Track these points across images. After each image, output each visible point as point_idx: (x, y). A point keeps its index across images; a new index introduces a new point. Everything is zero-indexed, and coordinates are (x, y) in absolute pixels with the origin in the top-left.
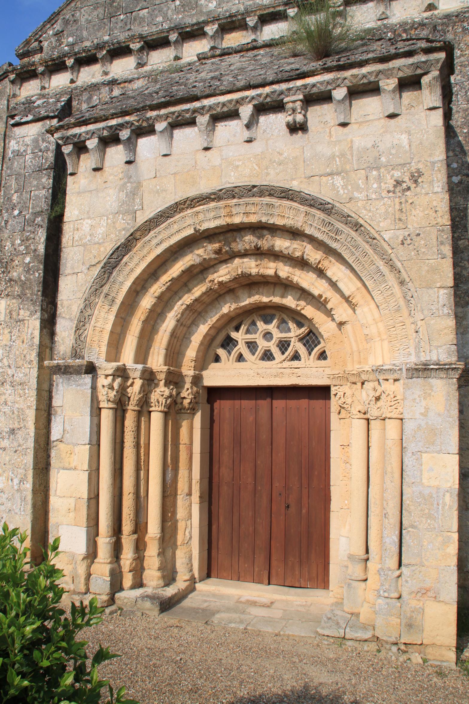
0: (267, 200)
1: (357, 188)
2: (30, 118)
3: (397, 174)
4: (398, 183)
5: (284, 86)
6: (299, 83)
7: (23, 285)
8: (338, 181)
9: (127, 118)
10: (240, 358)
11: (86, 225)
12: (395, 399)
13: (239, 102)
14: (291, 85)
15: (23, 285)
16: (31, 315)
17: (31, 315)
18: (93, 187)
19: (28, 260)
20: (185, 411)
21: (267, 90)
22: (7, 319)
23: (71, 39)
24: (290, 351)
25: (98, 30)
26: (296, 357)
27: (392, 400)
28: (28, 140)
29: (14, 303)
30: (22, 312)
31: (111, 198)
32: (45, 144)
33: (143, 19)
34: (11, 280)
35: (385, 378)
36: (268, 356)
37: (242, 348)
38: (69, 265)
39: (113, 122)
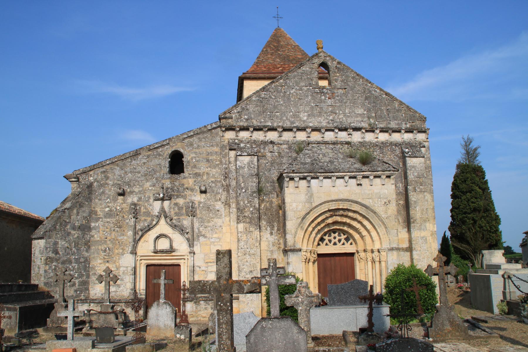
0: (350, 203)
1: (375, 203)
2: (246, 154)
3: (385, 200)
4: (385, 203)
5: (358, 173)
6: (362, 173)
7: (250, 218)
8: (371, 201)
9: (310, 174)
10: (327, 244)
11: (294, 205)
13: (345, 175)
14: (360, 173)
15: (250, 218)
16: (255, 229)
17: (255, 229)
18: (295, 192)
19: (251, 209)
21: (353, 174)
22: (245, 230)
23: (246, 117)
24: (342, 242)
25: (259, 116)
26: (343, 244)
28: (245, 162)
29: (248, 225)
30: (251, 228)
31: (303, 197)
32: (253, 166)
33: (277, 117)
34: (245, 216)
36: (335, 244)
37: (326, 241)
38: (289, 217)
39: (306, 174)
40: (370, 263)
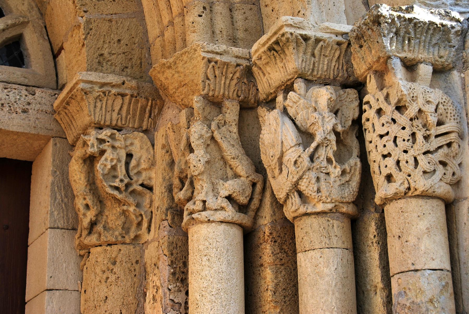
12: (442, 129)
27: (434, 131)
35: (410, 55)
40: (214, 253)
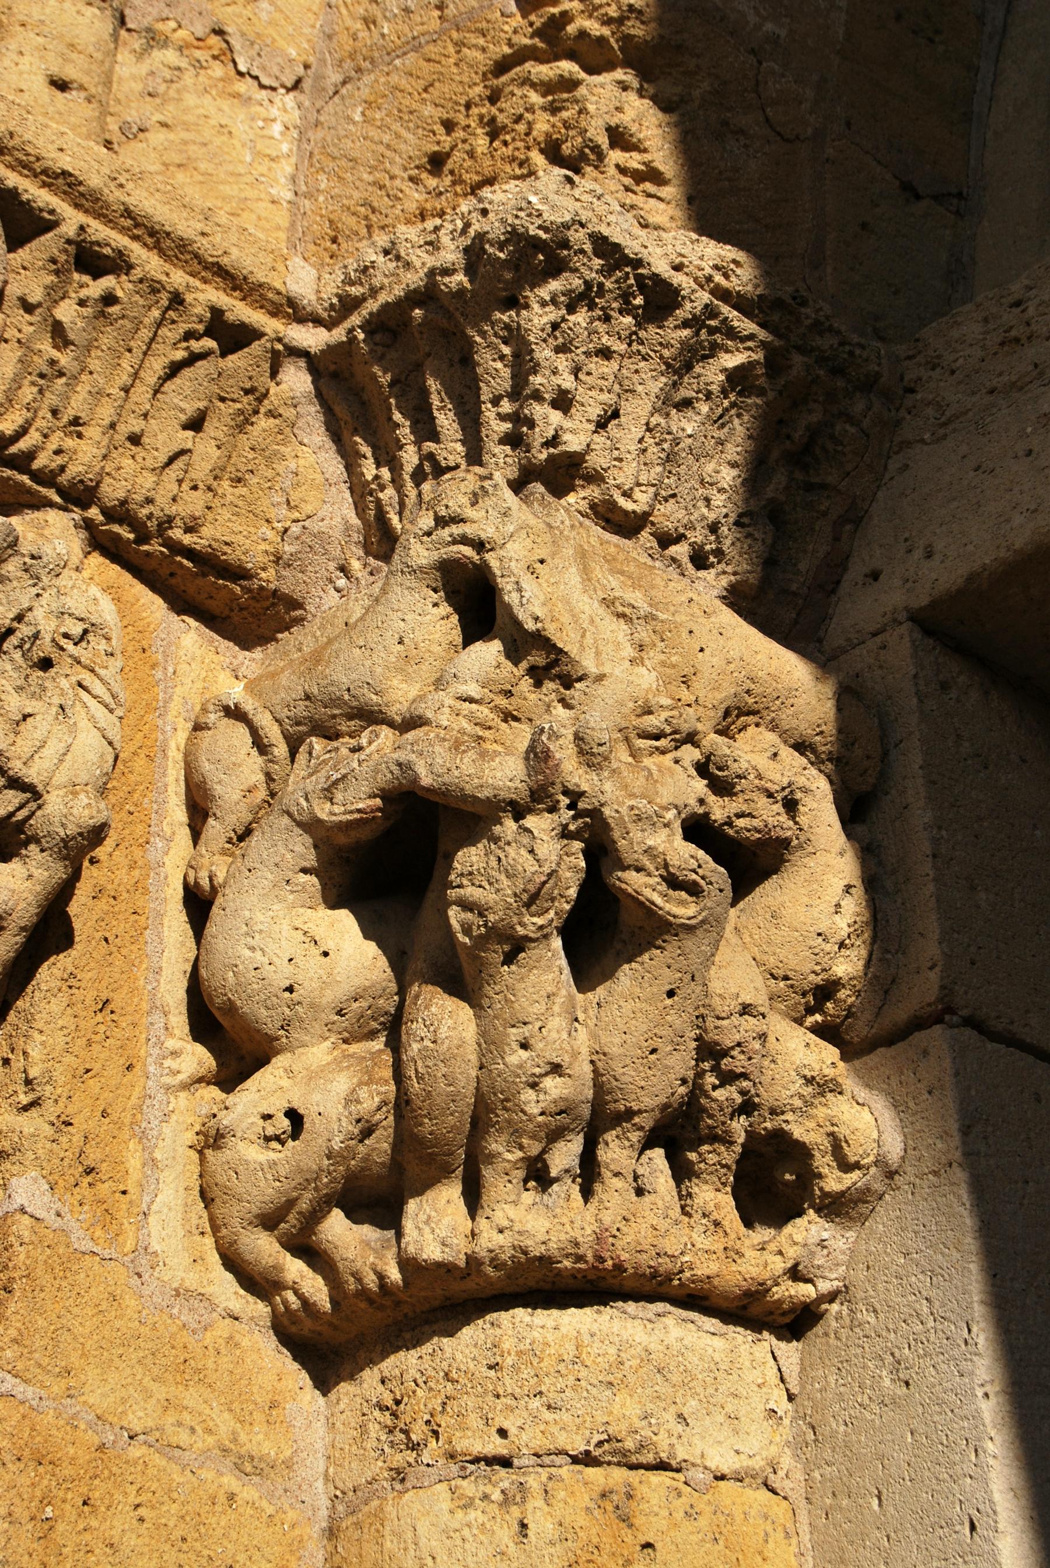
20: (527, 1221)
